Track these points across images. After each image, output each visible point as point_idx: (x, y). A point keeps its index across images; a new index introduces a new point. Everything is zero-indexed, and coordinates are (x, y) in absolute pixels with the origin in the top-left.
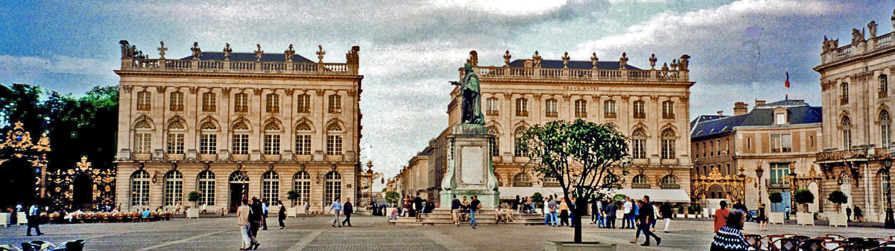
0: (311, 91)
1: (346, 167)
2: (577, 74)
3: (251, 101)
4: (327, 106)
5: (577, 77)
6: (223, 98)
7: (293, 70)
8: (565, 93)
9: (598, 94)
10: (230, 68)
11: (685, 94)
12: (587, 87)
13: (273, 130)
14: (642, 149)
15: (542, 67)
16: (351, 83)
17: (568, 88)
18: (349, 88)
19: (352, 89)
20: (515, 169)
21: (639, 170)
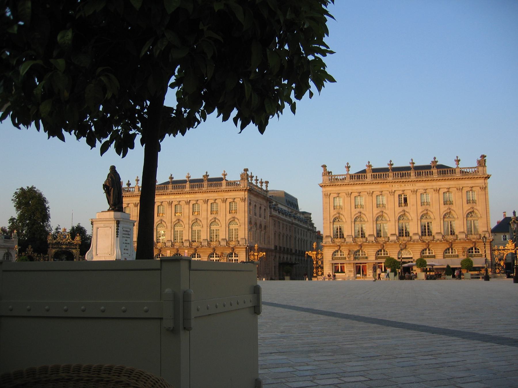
0: (218, 200)
1: (240, 250)
2: (399, 175)
3: (184, 208)
4: (228, 210)
5: (399, 177)
6: (168, 208)
7: (208, 187)
8: (390, 190)
9: (416, 188)
10: (172, 189)
11: (484, 184)
12: (406, 184)
13: (215, 226)
14: (428, 229)
15: (373, 172)
16: (243, 193)
17: (392, 186)
18: (241, 197)
19: (244, 197)
20: (354, 247)
21: (449, 244)
